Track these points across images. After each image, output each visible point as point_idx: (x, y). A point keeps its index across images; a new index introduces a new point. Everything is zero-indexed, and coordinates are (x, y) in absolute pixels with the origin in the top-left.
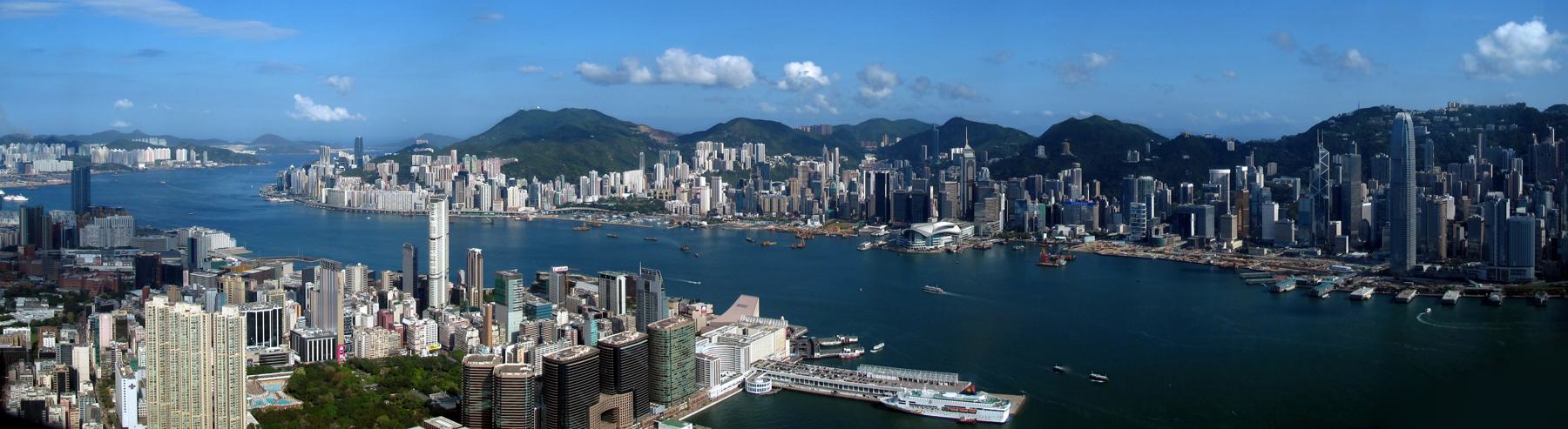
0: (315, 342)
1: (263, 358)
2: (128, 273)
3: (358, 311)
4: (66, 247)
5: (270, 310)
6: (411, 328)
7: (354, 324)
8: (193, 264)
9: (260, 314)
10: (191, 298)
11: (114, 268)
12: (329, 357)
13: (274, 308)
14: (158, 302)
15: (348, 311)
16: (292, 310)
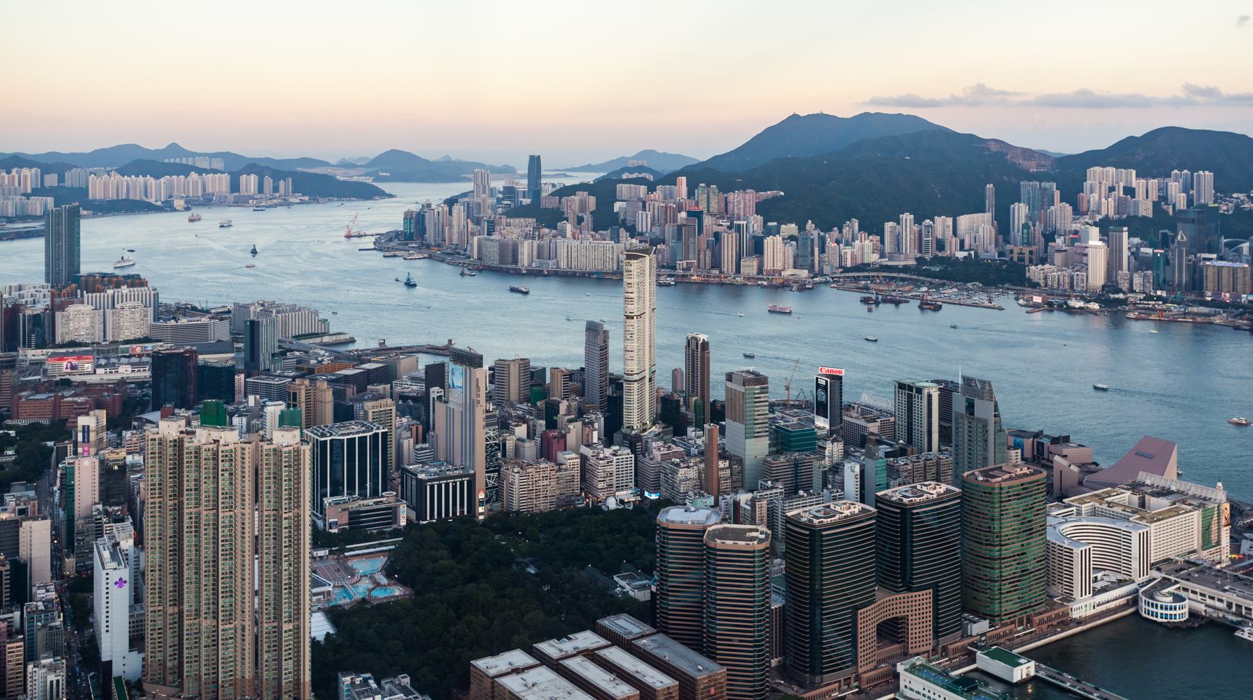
0: (440, 486)
1: (355, 516)
2: (141, 384)
3: (513, 433)
4: (30, 346)
5: (368, 434)
6: (592, 461)
7: (504, 455)
8: (252, 366)
9: (351, 441)
10: (244, 419)
11: (118, 377)
12: (462, 512)
13: (374, 431)
14: (169, 429)
15: (491, 434)
16: (406, 434)
